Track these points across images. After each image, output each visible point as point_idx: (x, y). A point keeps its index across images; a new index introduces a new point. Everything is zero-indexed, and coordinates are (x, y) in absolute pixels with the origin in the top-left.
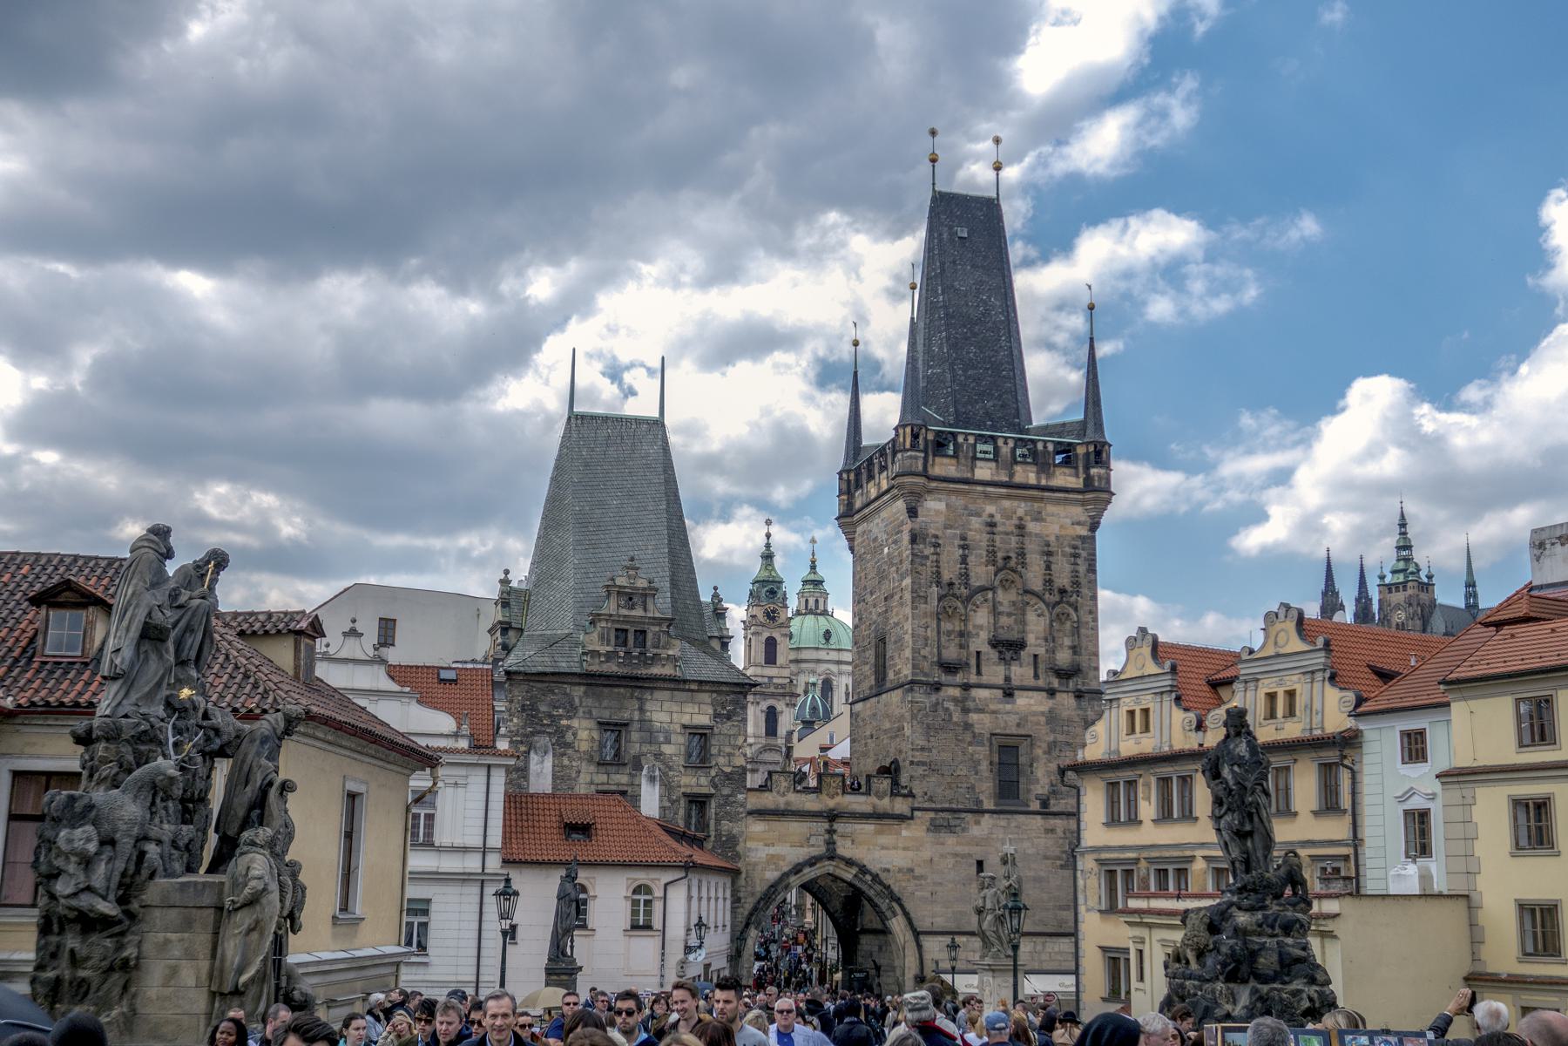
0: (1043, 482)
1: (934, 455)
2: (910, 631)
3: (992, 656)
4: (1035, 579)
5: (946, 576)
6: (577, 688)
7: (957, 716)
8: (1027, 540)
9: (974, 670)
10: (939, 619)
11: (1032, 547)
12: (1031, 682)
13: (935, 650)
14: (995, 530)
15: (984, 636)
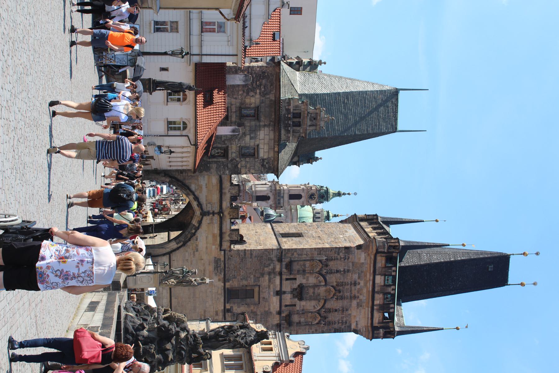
0: (375, 307)
1: (386, 256)
2: (304, 247)
3: (295, 285)
4: (332, 304)
5: (331, 263)
6: (273, 96)
7: (266, 269)
9: (288, 277)
11: (345, 303)
12: (283, 304)
13: (296, 259)
15: (304, 281)
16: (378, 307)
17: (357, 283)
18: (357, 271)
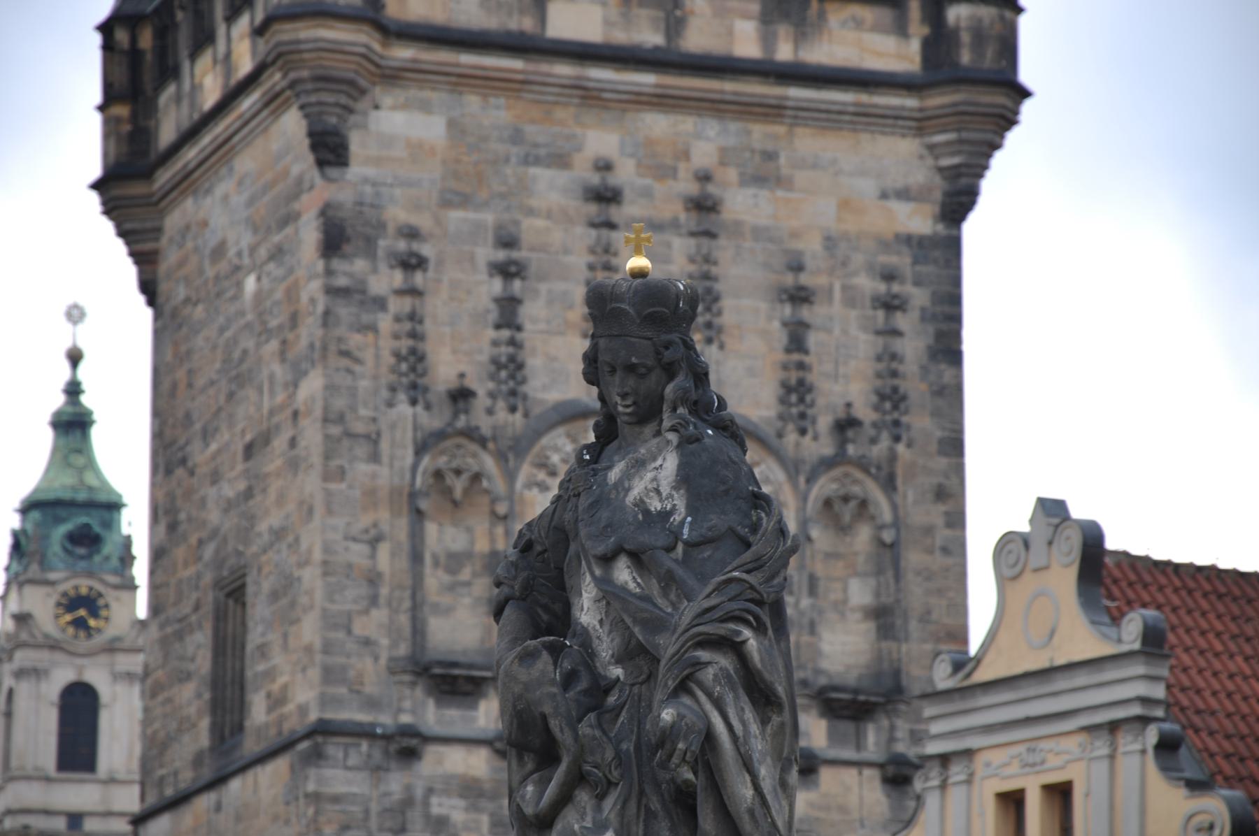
0: (785, 52)
2: (318, 555)
8: (724, 249)
10: (418, 515)
13: (404, 620)
14: (615, 213)
16: (784, 32)
17: (595, 179)
18: (508, 171)
